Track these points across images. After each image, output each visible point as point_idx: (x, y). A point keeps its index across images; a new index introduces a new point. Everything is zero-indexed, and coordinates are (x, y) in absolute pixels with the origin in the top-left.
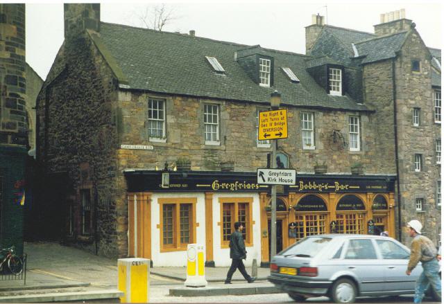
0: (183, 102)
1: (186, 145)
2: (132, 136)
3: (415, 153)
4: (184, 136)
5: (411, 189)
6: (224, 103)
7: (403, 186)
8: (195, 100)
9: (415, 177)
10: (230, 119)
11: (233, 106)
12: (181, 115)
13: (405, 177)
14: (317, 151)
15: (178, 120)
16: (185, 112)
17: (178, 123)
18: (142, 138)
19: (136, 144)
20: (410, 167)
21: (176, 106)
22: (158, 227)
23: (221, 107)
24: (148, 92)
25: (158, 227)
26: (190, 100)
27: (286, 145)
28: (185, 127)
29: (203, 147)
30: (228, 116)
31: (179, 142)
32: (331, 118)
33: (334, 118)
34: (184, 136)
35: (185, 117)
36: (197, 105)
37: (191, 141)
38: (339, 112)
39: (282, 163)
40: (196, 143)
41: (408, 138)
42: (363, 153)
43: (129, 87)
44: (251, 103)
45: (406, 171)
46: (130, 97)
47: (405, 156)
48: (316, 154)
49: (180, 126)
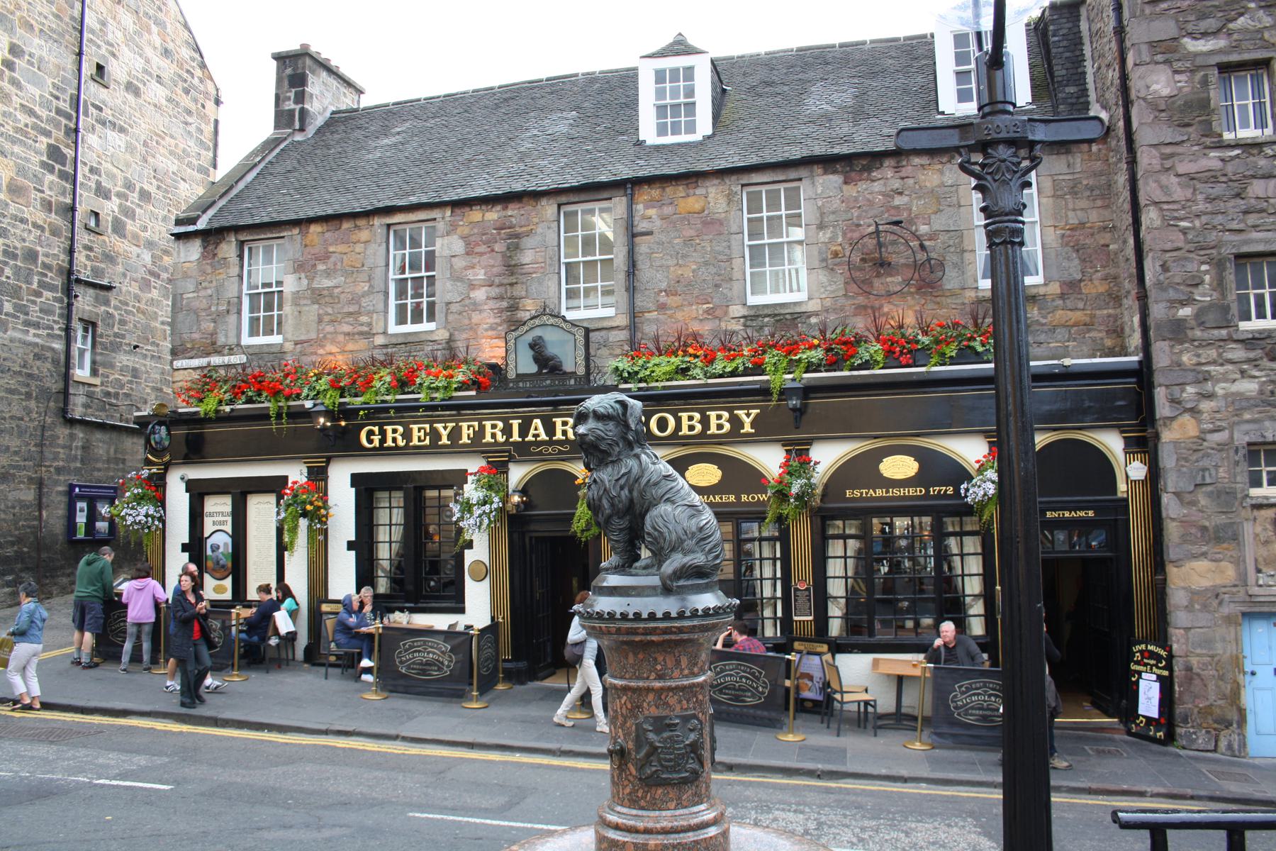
0: (328, 235)
1: (333, 342)
2: (196, 336)
3: (1227, 251)
4: (326, 318)
5: (1206, 406)
6: (448, 213)
7: (1160, 394)
8: (361, 222)
9: (1238, 353)
10: (467, 254)
11: (476, 215)
12: (321, 267)
13: (1162, 354)
14: (813, 306)
15: (311, 279)
16: (332, 259)
17: (313, 290)
18: (221, 340)
19: (208, 354)
20: (1197, 316)
21: (308, 249)
22: (183, 550)
23: (440, 226)
24: (237, 229)
25: (183, 550)
26: (346, 225)
27: (672, 301)
28: (331, 296)
29: (380, 340)
30: (458, 246)
31: (313, 335)
32: (877, 186)
33: (897, 184)
34: (326, 318)
35: (328, 274)
36: (364, 235)
37: (346, 328)
38: (917, 161)
39: (552, 358)
40: (361, 333)
41: (1179, 194)
42: (1055, 288)
43: (191, 228)
44: (536, 195)
45: (1177, 331)
46: (200, 250)
47: (1165, 268)
48: (809, 315)
49: (317, 296)
